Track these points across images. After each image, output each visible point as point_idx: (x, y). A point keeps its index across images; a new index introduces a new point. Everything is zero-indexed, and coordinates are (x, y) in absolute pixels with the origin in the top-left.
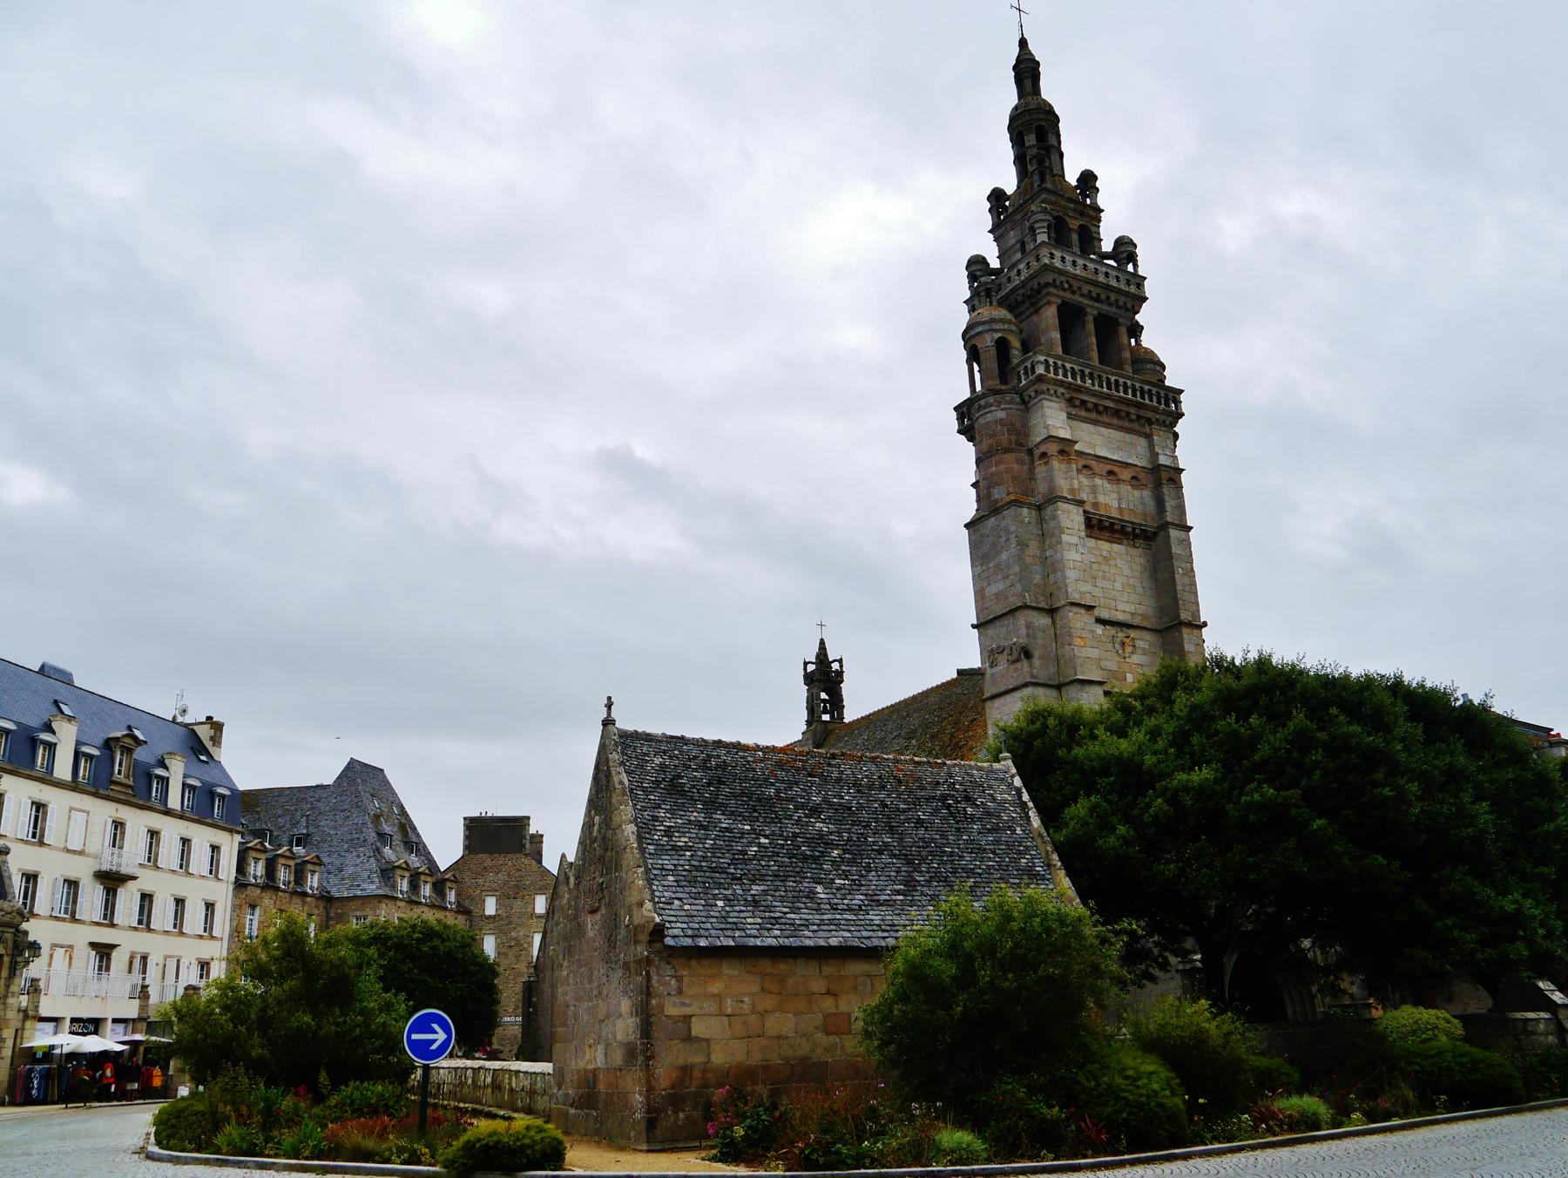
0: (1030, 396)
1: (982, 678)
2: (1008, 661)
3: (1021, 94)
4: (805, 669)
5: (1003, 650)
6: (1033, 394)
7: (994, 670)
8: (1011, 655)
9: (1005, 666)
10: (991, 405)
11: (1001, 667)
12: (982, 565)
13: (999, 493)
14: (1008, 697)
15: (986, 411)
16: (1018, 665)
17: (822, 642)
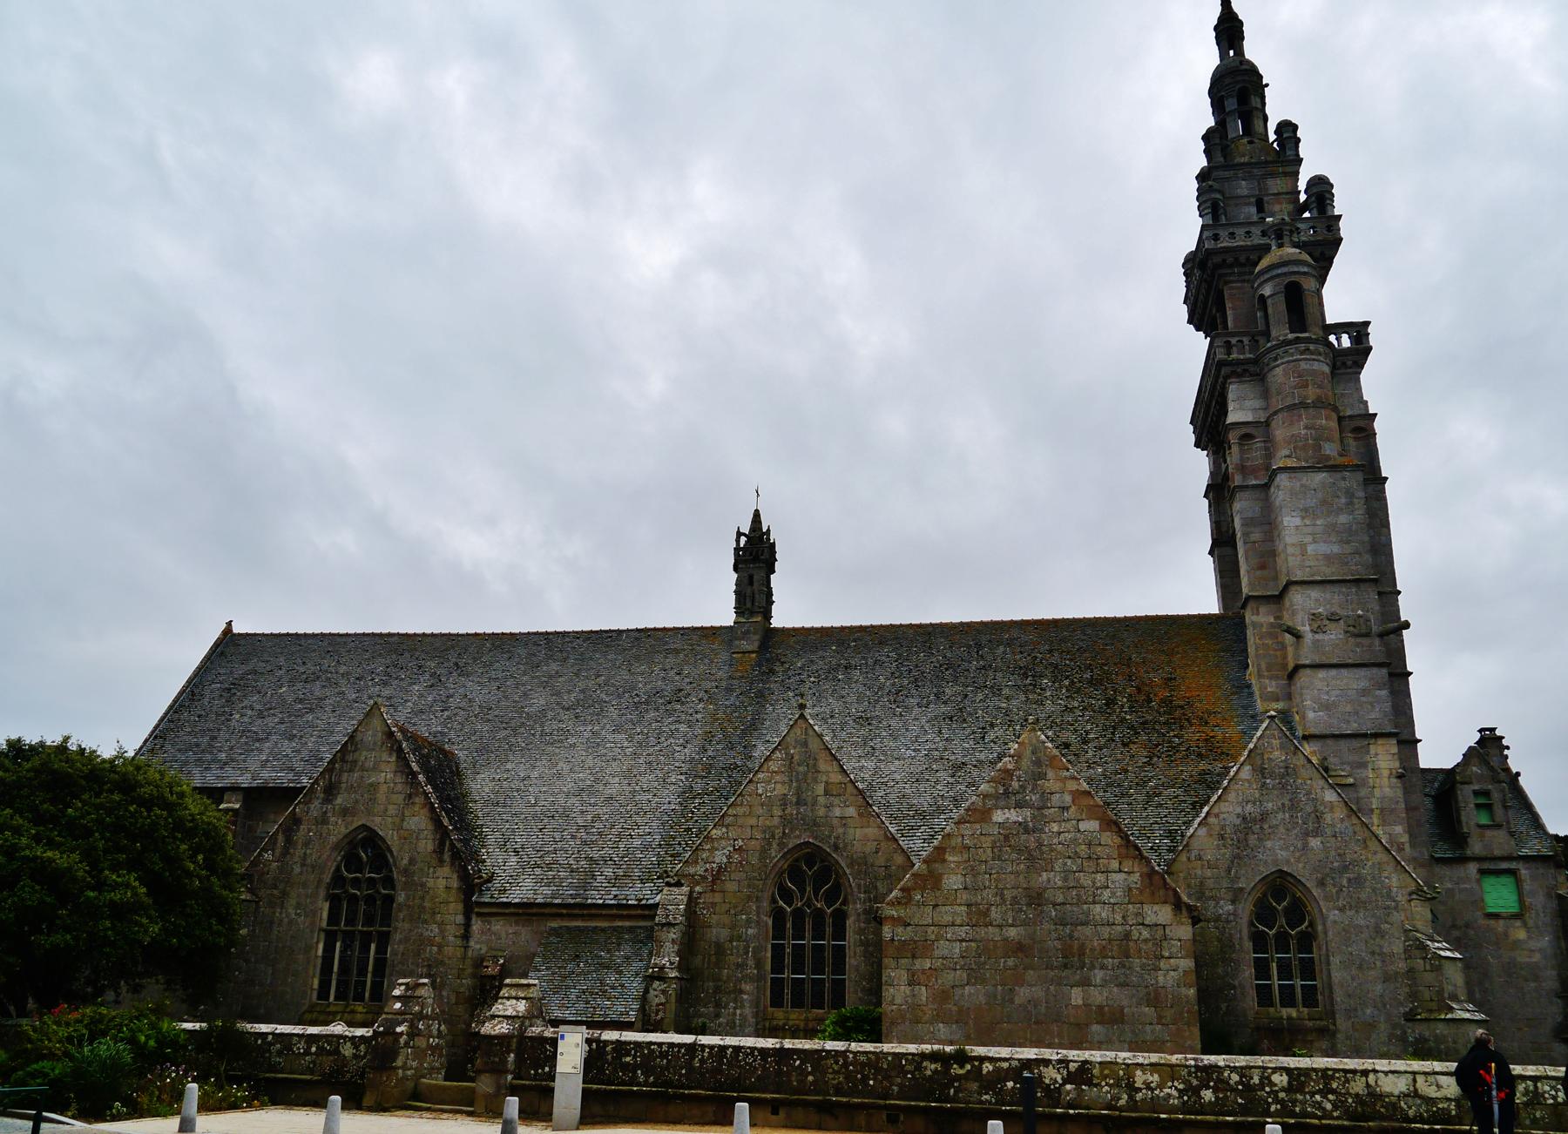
0: (1344, 364)
1: (1298, 642)
2: (1346, 632)
3: (1223, 54)
4: (738, 541)
5: (1340, 619)
6: (1349, 363)
7: (1319, 637)
8: (1354, 626)
9: (1341, 637)
10: (1320, 354)
11: (1333, 637)
12: (1303, 518)
13: (1331, 450)
14: (1344, 672)
15: (1313, 357)
16: (1365, 641)
17: (757, 515)
